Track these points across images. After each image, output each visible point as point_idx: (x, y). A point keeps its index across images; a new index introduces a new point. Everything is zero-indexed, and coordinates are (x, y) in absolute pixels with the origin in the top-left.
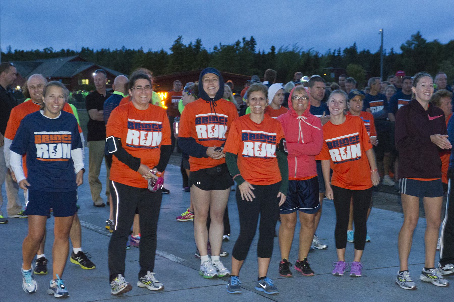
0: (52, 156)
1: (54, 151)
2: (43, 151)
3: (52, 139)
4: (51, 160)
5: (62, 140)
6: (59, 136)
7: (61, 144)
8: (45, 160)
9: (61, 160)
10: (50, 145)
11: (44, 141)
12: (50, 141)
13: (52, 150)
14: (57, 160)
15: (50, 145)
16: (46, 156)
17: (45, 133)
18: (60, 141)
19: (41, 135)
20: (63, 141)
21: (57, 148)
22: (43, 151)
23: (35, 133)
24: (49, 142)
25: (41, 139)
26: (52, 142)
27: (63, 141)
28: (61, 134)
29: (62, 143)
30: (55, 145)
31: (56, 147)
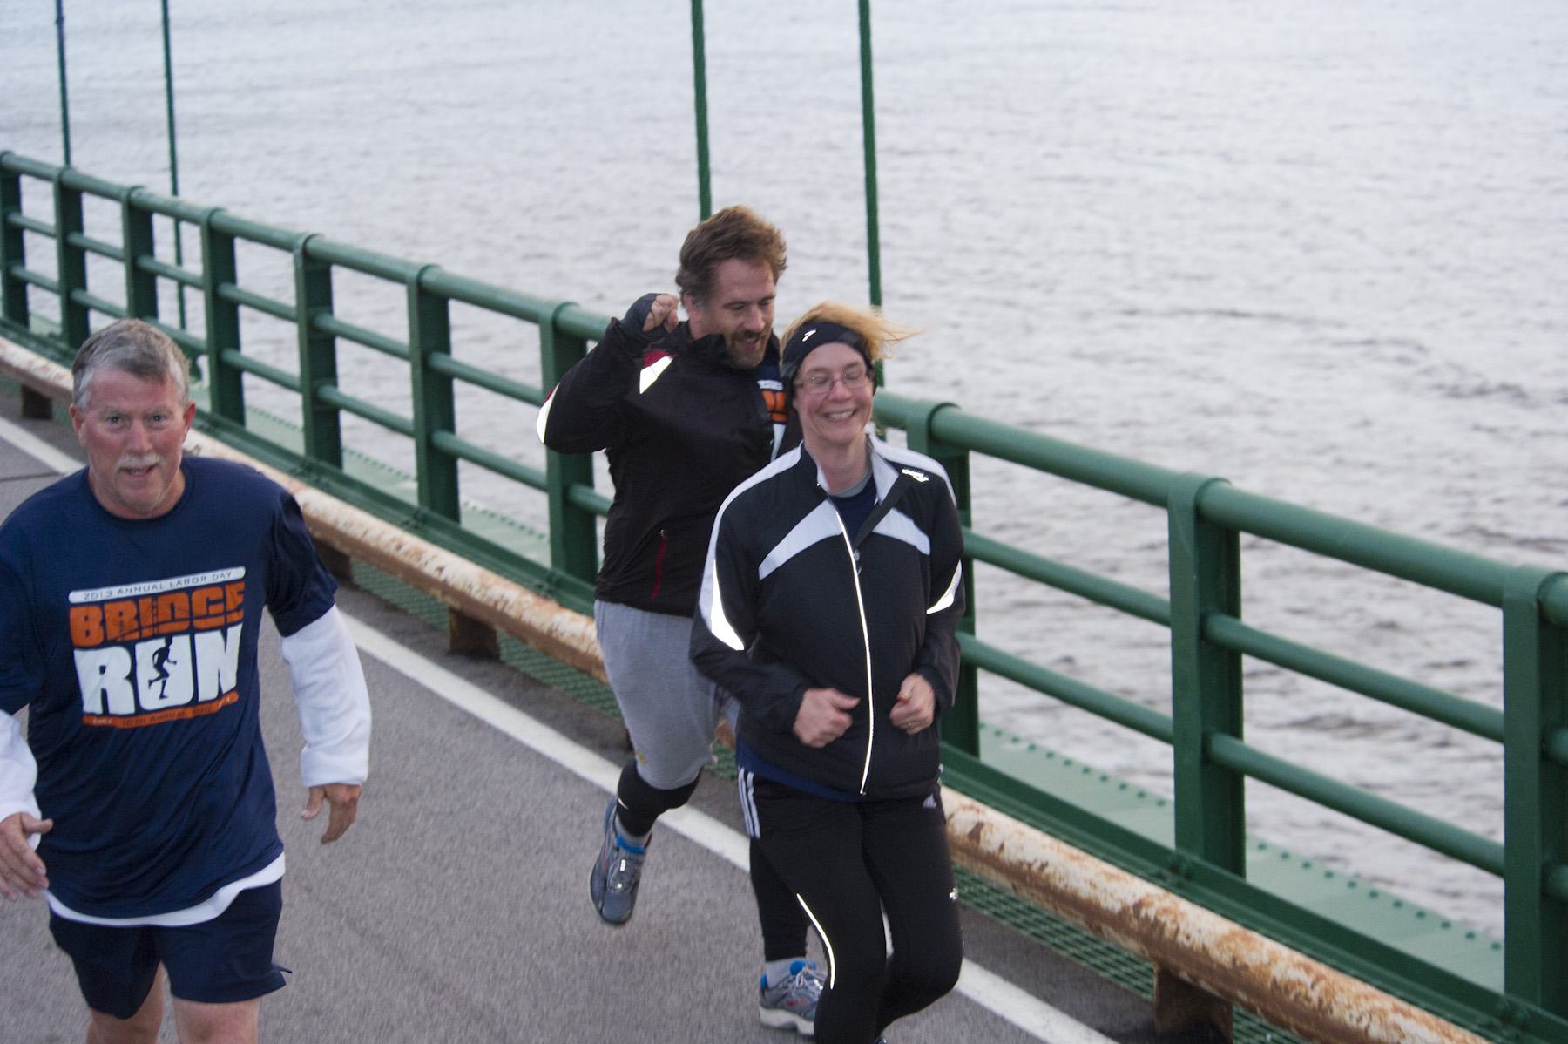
0: (151, 701)
1: (156, 674)
2: (107, 680)
4: (147, 720)
5: (191, 617)
7: (186, 639)
8: (120, 724)
9: (189, 713)
11: (113, 632)
12: (140, 629)
13: (146, 671)
14: (175, 715)
16: (122, 704)
17: (115, 592)
18: (185, 626)
19: (101, 604)
20: (197, 623)
21: (172, 656)
22: (107, 680)
23: (76, 597)
24: (136, 635)
26: (146, 632)
27: (197, 623)
28: (189, 591)
29: (192, 632)
30: (161, 643)
31: (163, 654)
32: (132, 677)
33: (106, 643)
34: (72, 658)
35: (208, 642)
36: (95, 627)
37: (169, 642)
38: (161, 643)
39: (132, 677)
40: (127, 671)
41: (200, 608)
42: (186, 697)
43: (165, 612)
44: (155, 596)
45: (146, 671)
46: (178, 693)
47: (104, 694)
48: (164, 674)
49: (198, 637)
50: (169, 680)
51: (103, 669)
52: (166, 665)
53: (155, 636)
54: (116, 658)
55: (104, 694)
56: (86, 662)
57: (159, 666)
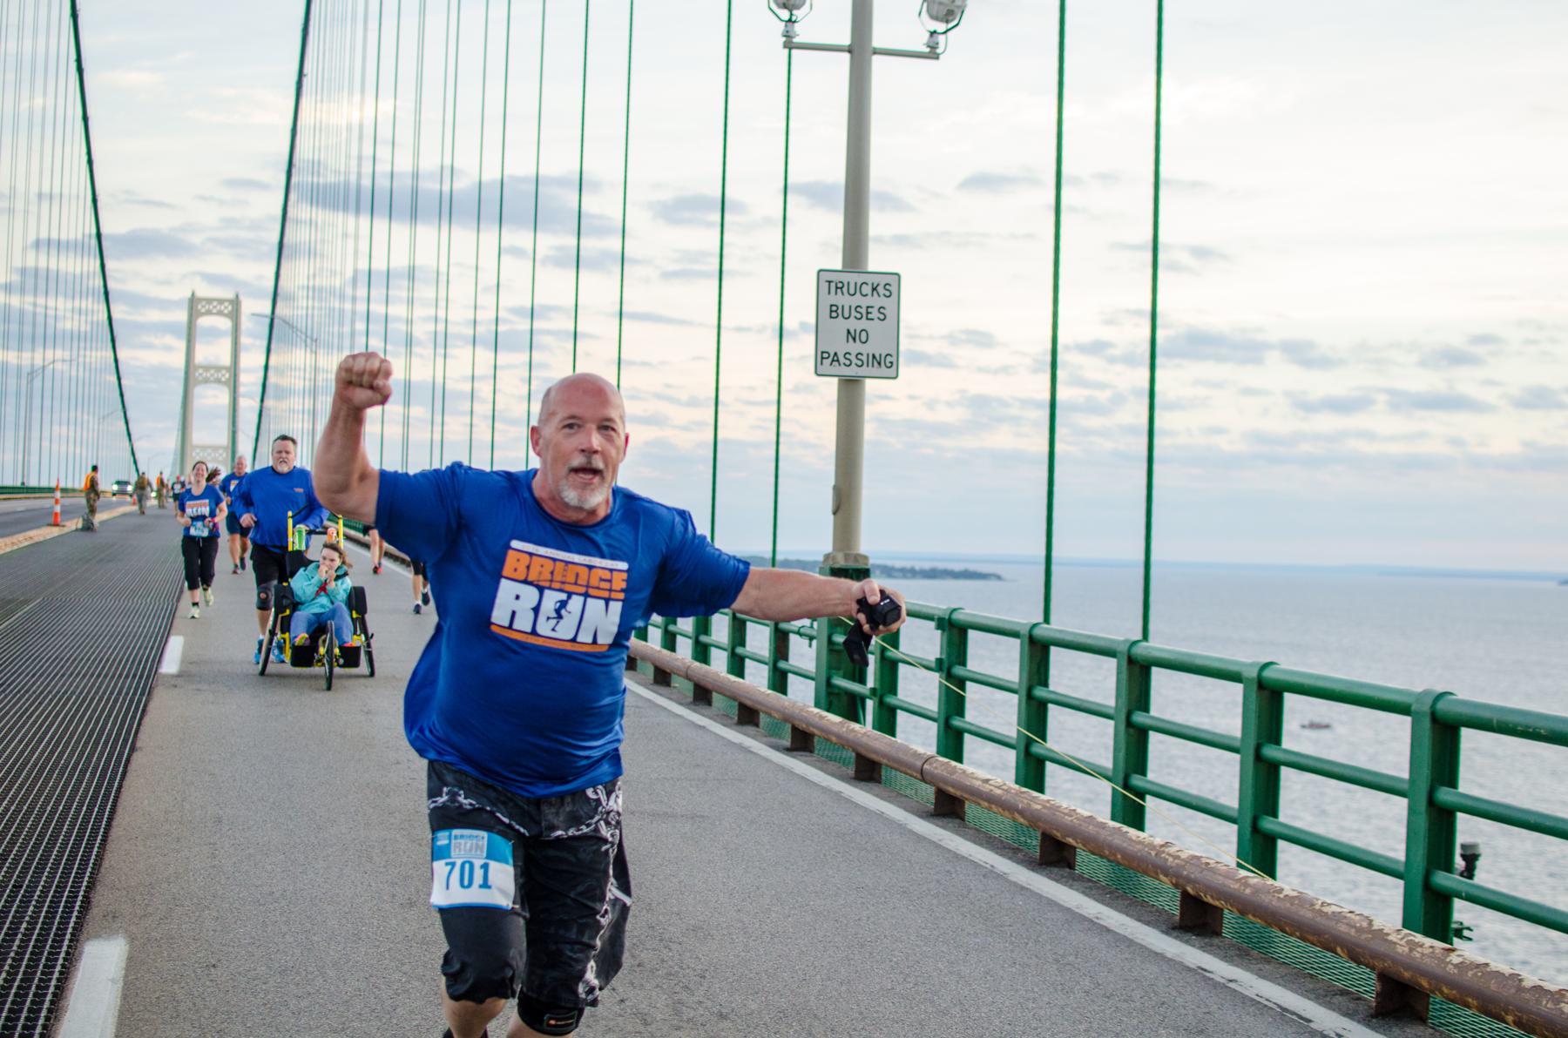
0: (544, 628)
2: (512, 604)
3: (558, 577)
7: (581, 599)
15: (547, 592)
17: (542, 550)
26: (557, 585)
30: (564, 596)
32: (536, 610)
33: (525, 582)
34: (498, 583)
38: (564, 596)
40: (534, 604)
42: (570, 636)
44: (567, 563)
46: (565, 630)
47: (514, 613)
48: (560, 617)
50: (562, 622)
51: (517, 597)
52: (563, 612)
53: (561, 590)
54: (530, 594)
55: (514, 613)
56: (506, 589)
57: (558, 611)
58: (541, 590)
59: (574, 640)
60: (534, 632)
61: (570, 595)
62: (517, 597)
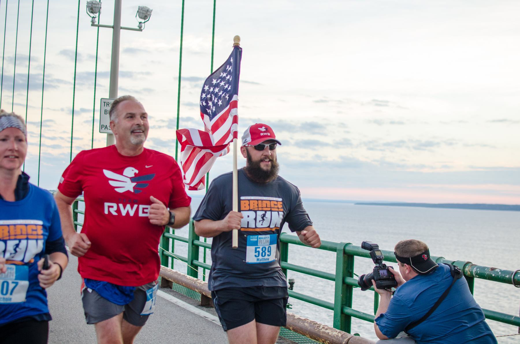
0: (259, 225)
3: (260, 206)
6: (268, 203)
7: (270, 212)
10: (258, 212)
13: (259, 218)
15: (258, 212)
17: (253, 198)
18: (270, 209)
21: (266, 216)
24: (257, 209)
25: (249, 205)
26: (260, 209)
27: (272, 209)
29: (271, 211)
30: (264, 212)
31: (264, 215)
32: (255, 219)
33: (250, 210)
35: (275, 214)
36: (247, 205)
37: (266, 212)
39: (255, 219)
40: (254, 217)
41: (273, 206)
43: (265, 206)
44: (262, 200)
45: (259, 218)
47: (248, 222)
48: (263, 220)
49: (273, 212)
51: (248, 216)
52: (264, 218)
54: (252, 214)
55: (248, 222)
57: (263, 218)
58: (256, 211)
59: (269, 227)
60: (256, 227)
61: (266, 211)
62: (248, 216)
